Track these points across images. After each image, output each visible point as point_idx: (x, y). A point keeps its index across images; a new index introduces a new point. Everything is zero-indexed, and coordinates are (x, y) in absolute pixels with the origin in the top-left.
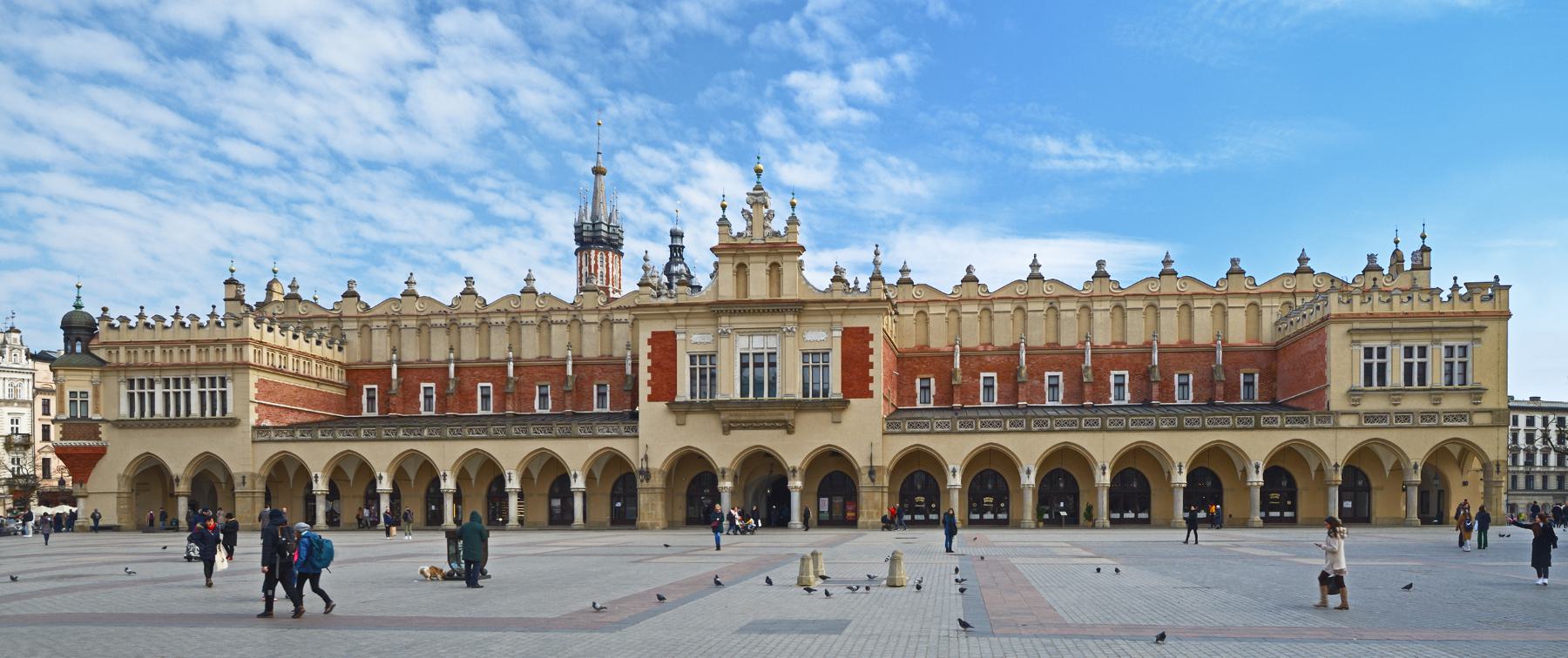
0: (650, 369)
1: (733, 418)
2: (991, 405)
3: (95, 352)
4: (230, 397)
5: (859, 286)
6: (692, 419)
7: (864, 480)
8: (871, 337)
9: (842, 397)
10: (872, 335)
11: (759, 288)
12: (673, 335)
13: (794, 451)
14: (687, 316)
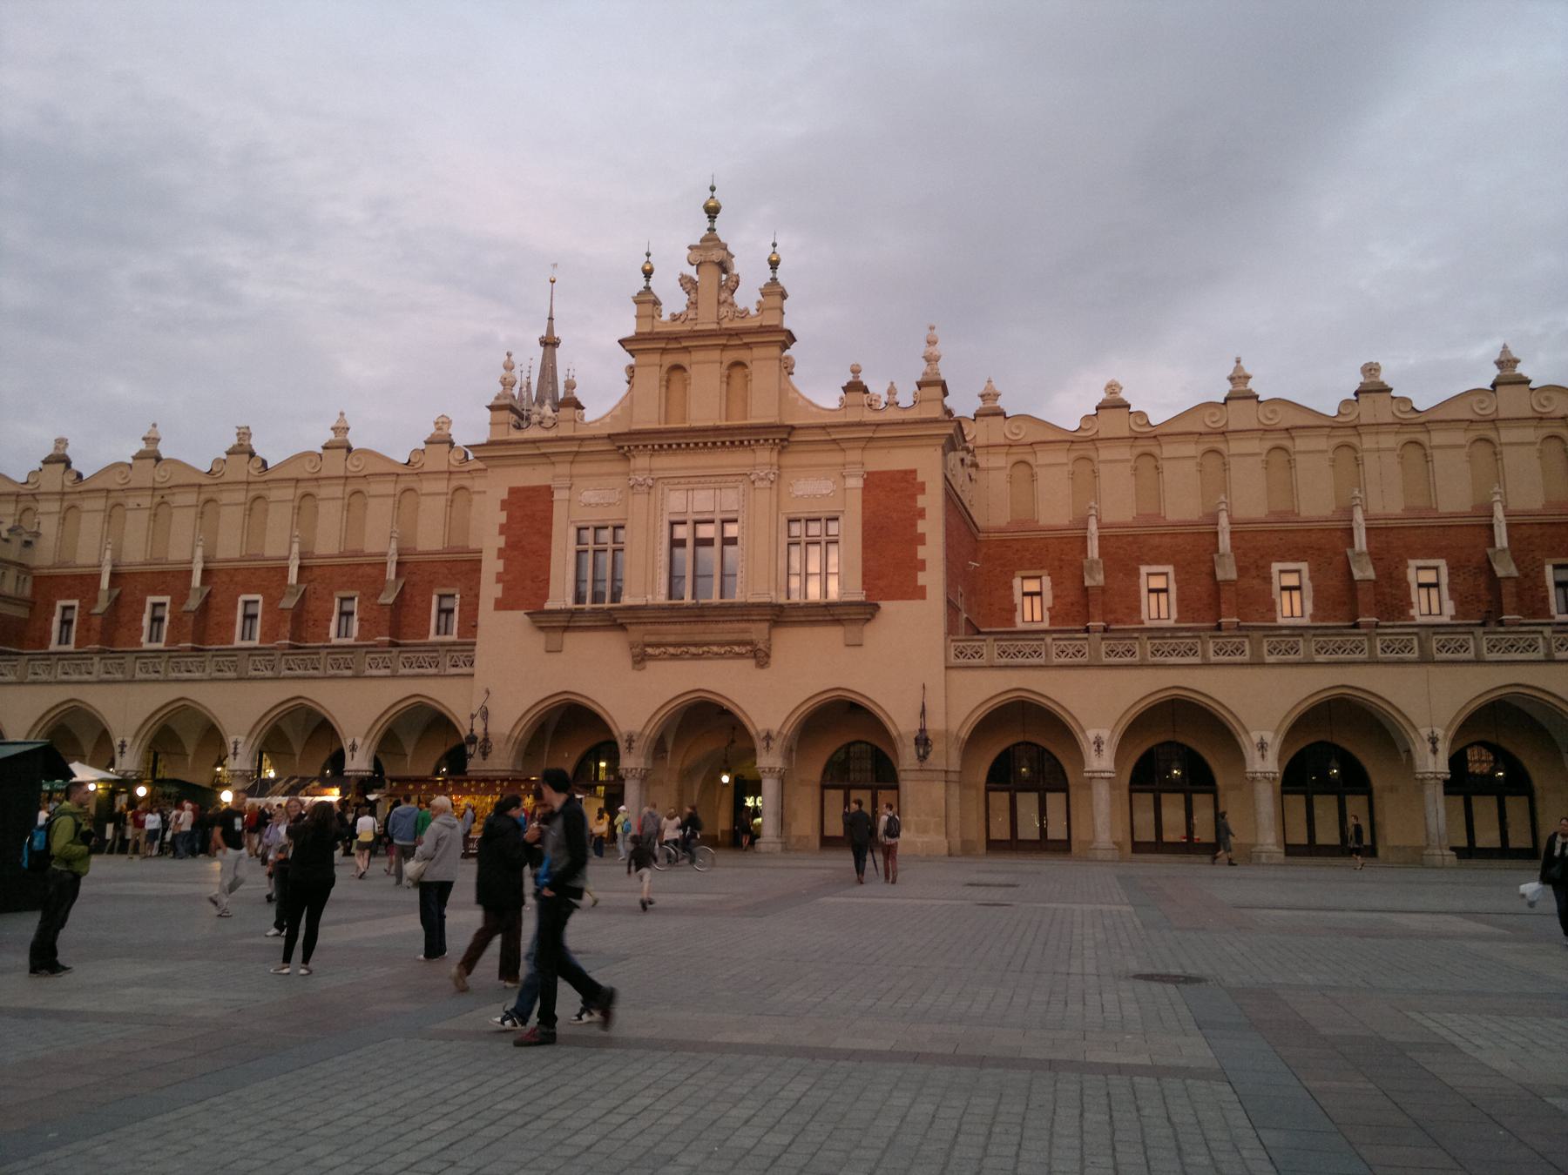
0: (501, 553)
1: (653, 639)
7: (907, 758)
8: (922, 488)
9: (864, 599)
10: (923, 484)
12: (548, 491)
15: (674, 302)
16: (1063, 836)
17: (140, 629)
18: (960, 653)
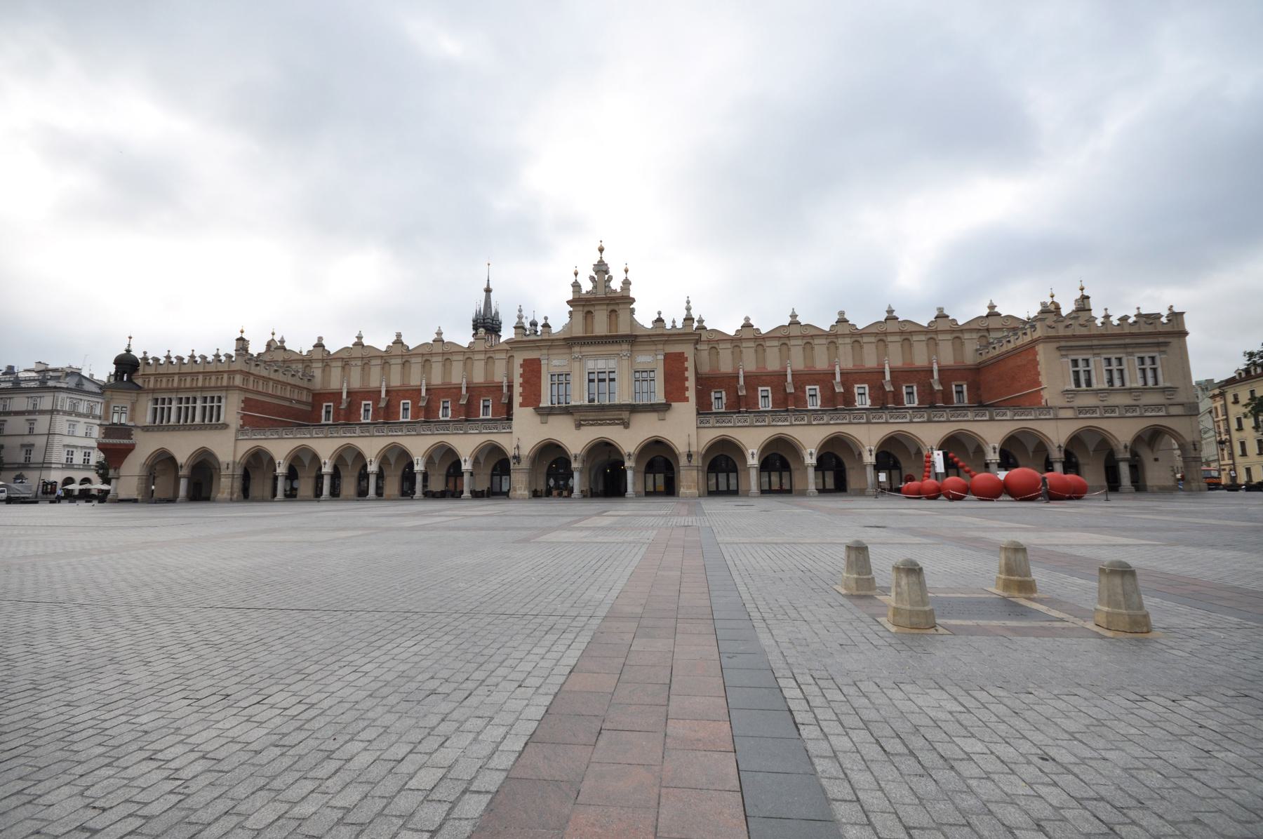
0: (521, 385)
2: (767, 409)
3: (136, 381)
4: (223, 410)
5: (676, 324)
6: (554, 420)
7: (683, 461)
8: (686, 359)
9: (664, 402)
11: (601, 326)
12: (539, 360)
13: (629, 440)
14: (550, 347)
15: (587, 286)
16: (735, 489)
17: (360, 415)
18: (701, 422)
